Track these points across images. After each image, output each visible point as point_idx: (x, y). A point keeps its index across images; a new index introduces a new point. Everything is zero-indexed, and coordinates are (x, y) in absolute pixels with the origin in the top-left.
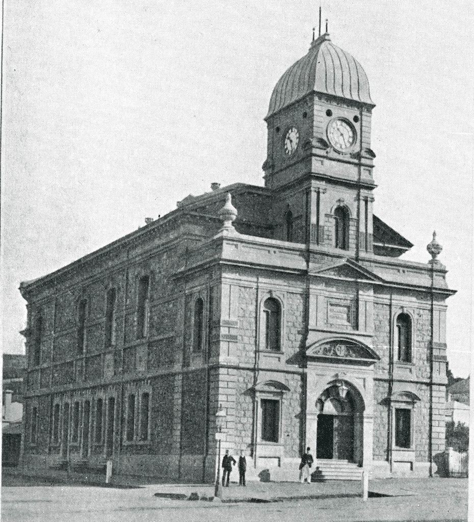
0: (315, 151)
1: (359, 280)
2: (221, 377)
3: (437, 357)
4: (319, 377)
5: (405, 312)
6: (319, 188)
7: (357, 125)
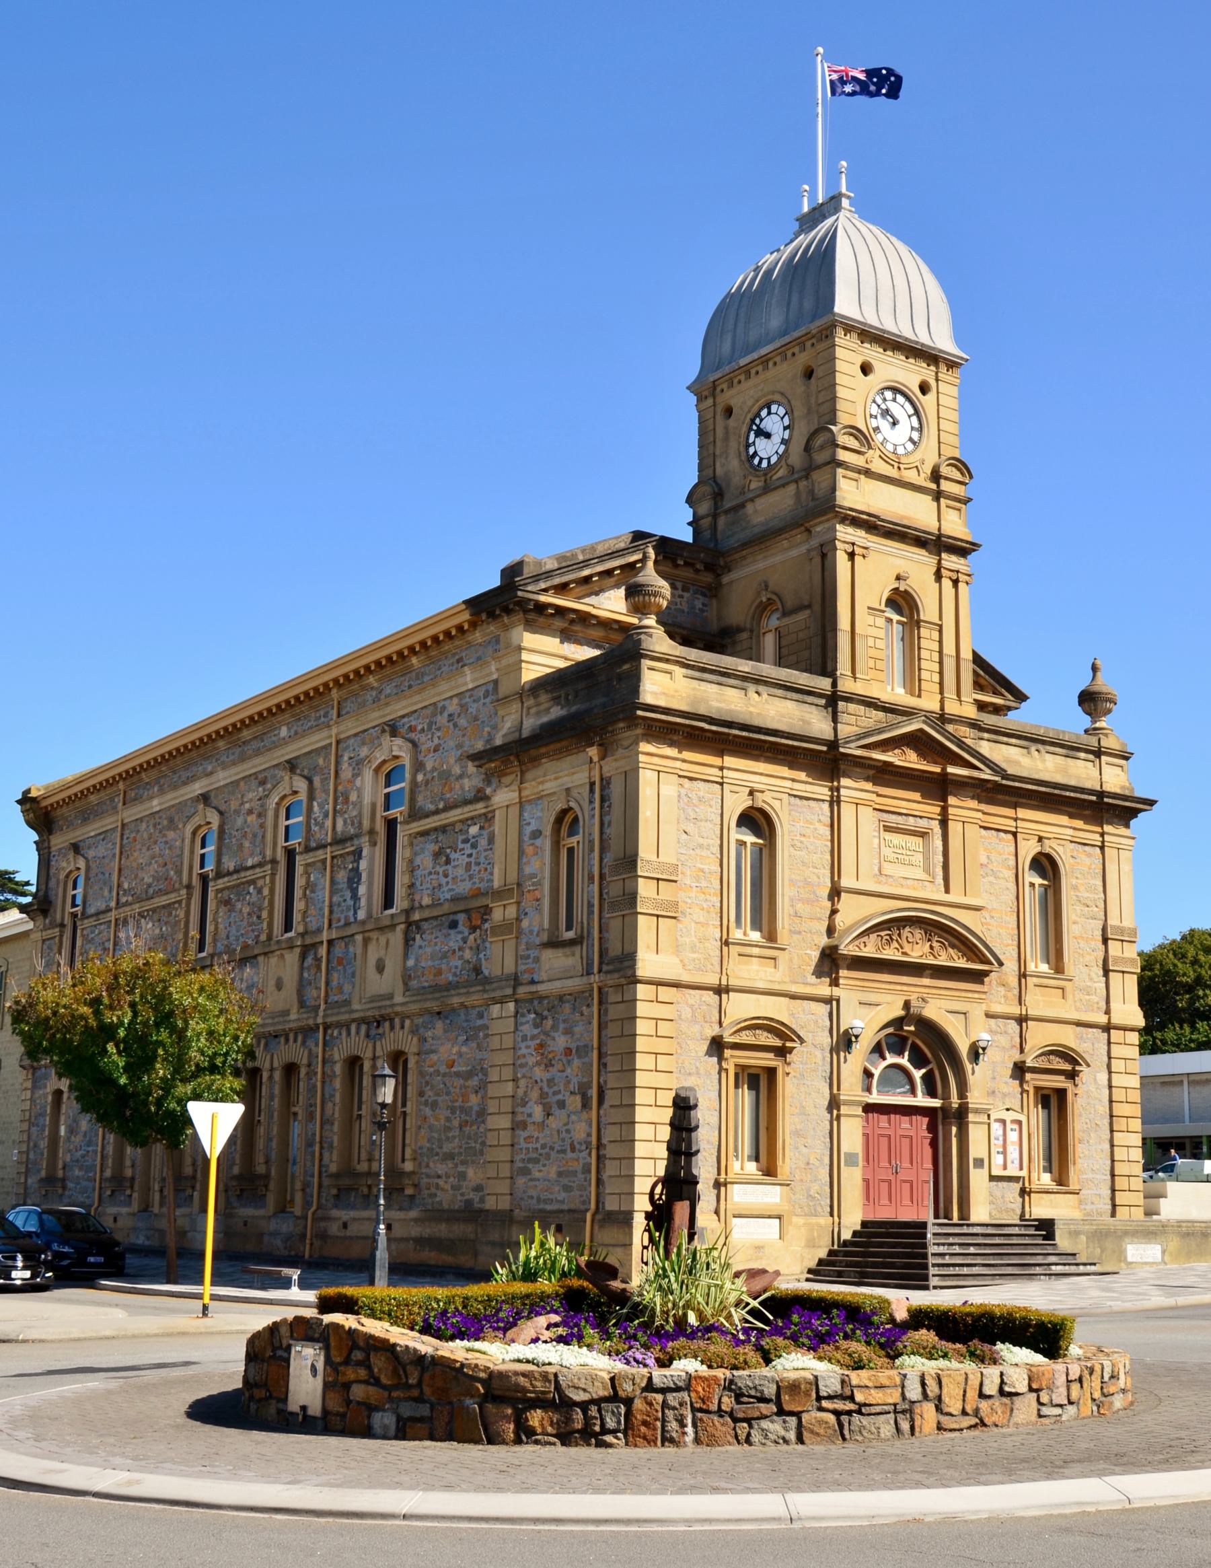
0: (842, 455)
1: (951, 770)
2: (642, 1009)
3: (1116, 959)
4: (869, 1008)
5: (1047, 850)
6: (853, 544)
7: (928, 401)
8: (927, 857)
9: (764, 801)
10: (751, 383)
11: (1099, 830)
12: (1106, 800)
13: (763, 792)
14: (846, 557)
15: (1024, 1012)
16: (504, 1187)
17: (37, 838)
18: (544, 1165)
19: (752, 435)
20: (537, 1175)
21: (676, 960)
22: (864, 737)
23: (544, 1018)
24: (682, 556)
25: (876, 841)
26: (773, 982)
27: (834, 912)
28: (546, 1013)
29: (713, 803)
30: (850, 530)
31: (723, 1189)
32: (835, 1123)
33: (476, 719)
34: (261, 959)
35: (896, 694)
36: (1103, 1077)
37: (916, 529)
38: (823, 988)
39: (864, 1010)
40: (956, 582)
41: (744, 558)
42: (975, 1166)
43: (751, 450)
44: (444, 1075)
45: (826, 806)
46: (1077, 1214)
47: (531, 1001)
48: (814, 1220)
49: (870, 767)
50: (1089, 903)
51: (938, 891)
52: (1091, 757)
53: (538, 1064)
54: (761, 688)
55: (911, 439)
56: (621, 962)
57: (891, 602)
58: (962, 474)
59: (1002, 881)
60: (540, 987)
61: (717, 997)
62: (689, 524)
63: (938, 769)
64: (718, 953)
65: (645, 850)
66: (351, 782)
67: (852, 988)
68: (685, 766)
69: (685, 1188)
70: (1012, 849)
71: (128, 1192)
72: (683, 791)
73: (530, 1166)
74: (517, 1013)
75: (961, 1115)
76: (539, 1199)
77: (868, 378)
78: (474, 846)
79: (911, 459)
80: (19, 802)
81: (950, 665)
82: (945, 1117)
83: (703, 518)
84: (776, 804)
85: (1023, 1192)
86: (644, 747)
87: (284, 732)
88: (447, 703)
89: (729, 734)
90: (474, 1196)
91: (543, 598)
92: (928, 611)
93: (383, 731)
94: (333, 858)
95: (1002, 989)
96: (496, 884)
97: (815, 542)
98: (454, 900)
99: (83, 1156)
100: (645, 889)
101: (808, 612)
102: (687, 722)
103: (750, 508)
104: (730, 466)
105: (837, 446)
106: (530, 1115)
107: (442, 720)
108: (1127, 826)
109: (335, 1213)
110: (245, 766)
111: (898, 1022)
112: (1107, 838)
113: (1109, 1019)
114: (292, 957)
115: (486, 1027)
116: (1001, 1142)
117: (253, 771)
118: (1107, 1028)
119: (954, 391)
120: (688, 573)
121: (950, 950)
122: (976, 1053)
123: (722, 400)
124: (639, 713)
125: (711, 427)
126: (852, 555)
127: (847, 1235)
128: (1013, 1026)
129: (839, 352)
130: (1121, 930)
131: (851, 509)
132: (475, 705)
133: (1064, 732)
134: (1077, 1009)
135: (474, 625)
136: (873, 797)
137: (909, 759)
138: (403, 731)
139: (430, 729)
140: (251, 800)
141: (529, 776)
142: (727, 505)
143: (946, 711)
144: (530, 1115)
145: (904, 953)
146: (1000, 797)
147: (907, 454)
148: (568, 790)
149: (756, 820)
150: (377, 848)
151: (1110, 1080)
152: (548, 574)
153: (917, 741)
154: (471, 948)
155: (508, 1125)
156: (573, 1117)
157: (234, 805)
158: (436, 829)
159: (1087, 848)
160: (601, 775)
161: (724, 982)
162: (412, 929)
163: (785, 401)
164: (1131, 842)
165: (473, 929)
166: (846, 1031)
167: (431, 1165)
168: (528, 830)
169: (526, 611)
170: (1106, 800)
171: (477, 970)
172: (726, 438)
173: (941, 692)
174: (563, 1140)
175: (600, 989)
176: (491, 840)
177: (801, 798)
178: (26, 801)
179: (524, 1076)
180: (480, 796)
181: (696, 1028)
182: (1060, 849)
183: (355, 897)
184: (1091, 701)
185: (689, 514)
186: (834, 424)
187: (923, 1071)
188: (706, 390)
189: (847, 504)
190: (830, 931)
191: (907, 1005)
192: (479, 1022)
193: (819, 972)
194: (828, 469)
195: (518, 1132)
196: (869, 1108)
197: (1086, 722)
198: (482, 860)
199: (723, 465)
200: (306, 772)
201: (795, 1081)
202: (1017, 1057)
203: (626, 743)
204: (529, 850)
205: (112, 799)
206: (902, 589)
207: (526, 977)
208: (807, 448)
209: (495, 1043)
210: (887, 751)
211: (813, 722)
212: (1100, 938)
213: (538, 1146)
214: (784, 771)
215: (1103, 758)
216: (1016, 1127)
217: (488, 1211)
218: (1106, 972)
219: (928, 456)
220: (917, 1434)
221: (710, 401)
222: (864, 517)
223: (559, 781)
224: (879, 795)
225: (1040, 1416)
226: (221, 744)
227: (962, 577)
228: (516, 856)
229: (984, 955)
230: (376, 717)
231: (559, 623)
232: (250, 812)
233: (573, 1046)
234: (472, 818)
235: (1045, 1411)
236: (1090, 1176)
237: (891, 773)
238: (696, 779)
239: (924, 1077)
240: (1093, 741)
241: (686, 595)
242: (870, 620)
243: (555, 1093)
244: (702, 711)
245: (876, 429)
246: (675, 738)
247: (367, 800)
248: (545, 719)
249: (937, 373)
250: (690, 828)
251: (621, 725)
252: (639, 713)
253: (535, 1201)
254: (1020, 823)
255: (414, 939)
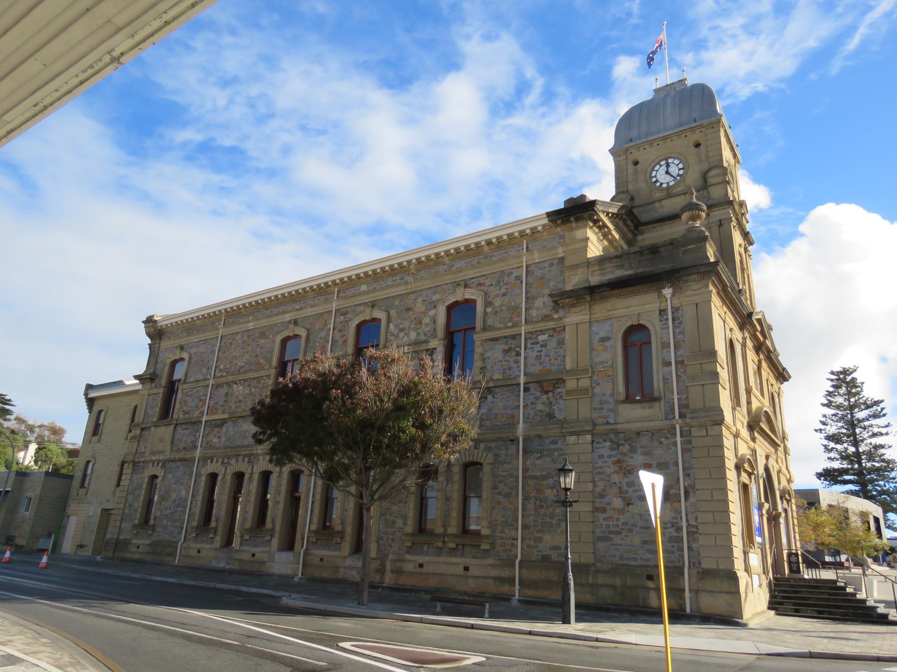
17: (150, 342)
20: (619, 542)
33: (542, 278)
53: (615, 472)
71: (211, 535)
73: (612, 536)
74: (593, 441)
76: (621, 558)
96: (568, 367)
99: (171, 513)
106: (610, 504)
109: (408, 557)
141: (594, 307)
144: (610, 504)
148: (639, 314)
155: (590, 509)
168: (596, 338)
176: (561, 343)
178: (149, 322)
179: (601, 480)
198: (552, 353)
213: (620, 523)
221: (624, 157)
234: (541, 331)
243: (634, 491)
253: (618, 558)
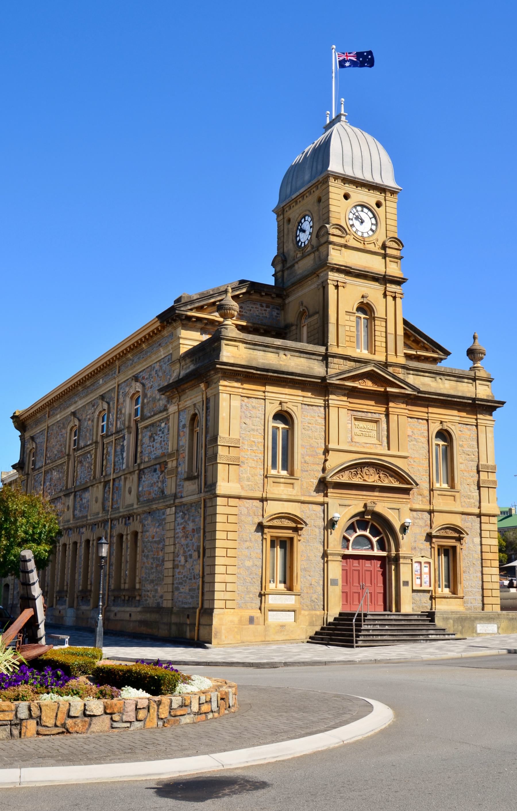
0: (332, 239)
1: (389, 389)
2: (219, 509)
3: (484, 481)
4: (344, 508)
6: (337, 281)
8: (378, 433)
9: (287, 407)
10: (297, 207)
11: (475, 417)
12: (477, 402)
13: (286, 403)
14: (334, 287)
15: (432, 508)
16: (169, 596)
17: (20, 434)
18: (184, 586)
19: (298, 232)
20: (182, 590)
21: (239, 486)
22: (340, 375)
23: (185, 514)
24: (264, 291)
25: (350, 425)
26: (294, 495)
27: (326, 460)
28: (186, 512)
29: (260, 409)
30: (336, 274)
31: (263, 597)
32: (326, 564)
34: (90, 488)
35: (363, 353)
36: (477, 540)
37: (372, 273)
38: (320, 498)
39: (343, 508)
40: (394, 298)
41: (294, 290)
42: (404, 585)
43: (298, 239)
44: (151, 542)
45: (322, 409)
46: (461, 609)
47: (181, 506)
48: (314, 612)
49: (345, 389)
50: (470, 453)
51: (384, 449)
52: (471, 381)
54: (286, 353)
55: (371, 230)
56: (211, 487)
57: (359, 309)
58: (399, 245)
59: (421, 444)
60: (183, 500)
61: (261, 503)
62: (273, 275)
63: (382, 389)
64: (262, 481)
65: (223, 432)
66: (122, 404)
67: (335, 498)
68: (244, 391)
69: (30, 602)
70: (426, 427)
72: (244, 403)
73: (179, 586)
74: (176, 512)
75: (396, 560)
77: (349, 200)
78: (163, 433)
79: (371, 239)
80: (12, 418)
81: (391, 338)
82: (389, 561)
83: (278, 272)
84: (294, 409)
85: (432, 598)
86: (222, 382)
87: (101, 382)
88: (155, 365)
89: (268, 375)
90: (159, 600)
91: (189, 313)
92: (379, 312)
93: (132, 380)
94: (116, 440)
95: (420, 497)
97: (320, 281)
98: (156, 458)
100: (222, 451)
101: (318, 315)
102: (244, 370)
103: (296, 266)
104: (290, 247)
105: (330, 234)
106: (180, 561)
107: (153, 373)
108: (491, 415)
110: (88, 398)
111: (361, 514)
112: (479, 421)
113: (480, 511)
114: (101, 486)
115: (165, 519)
116: (419, 573)
117: (90, 400)
118: (479, 515)
119: (395, 205)
120: (268, 299)
121: (390, 478)
122: (404, 528)
123: (287, 215)
124: (218, 366)
125: (282, 229)
126: (337, 287)
127: (331, 620)
128: (426, 515)
129: (331, 189)
130: (488, 467)
131: (335, 264)
132: (165, 366)
133: (455, 369)
134: (462, 506)
135: (163, 327)
136: (348, 404)
137: (368, 385)
138: (140, 379)
139: (149, 378)
140: (90, 414)
141: (182, 398)
142: (288, 265)
143: (388, 361)
145: (364, 480)
146: (419, 402)
147: (369, 236)
149: (284, 416)
150: (132, 435)
151: (481, 541)
152: (192, 302)
153: (371, 376)
154: (161, 481)
155: (171, 566)
156: (195, 563)
157: (84, 416)
158: (150, 425)
159: (468, 426)
160: (206, 397)
161: (264, 496)
162: (141, 472)
163: (310, 214)
164: (493, 423)
165: (162, 472)
166: (331, 519)
167: (146, 586)
168: (182, 424)
169: (182, 320)
170: (477, 402)
171: (163, 492)
172: (288, 234)
173: (386, 352)
174: (191, 574)
175: (204, 500)
177: (308, 405)
178: (14, 418)
180: (165, 409)
181: (250, 518)
182: (453, 427)
183: (123, 459)
184: (473, 354)
185: (272, 271)
186: (328, 224)
187: (378, 538)
188: (280, 211)
189: (334, 262)
190: (324, 470)
191: (365, 506)
192: (163, 517)
193: (318, 490)
194: (325, 245)
195: (176, 570)
196: (345, 557)
197: (470, 364)
198: (165, 439)
199: (287, 247)
200: (108, 400)
201: (304, 544)
202: (428, 530)
203: (215, 381)
204: (181, 434)
205: (45, 415)
206: (365, 302)
207: (179, 495)
208: (317, 236)
209: (168, 527)
210: (356, 381)
211: (317, 368)
212: (476, 471)
213: (182, 576)
214: (299, 392)
215: (477, 382)
216: (427, 565)
217: (164, 608)
218: (479, 488)
219: (381, 237)
220: (22, 737)
221: (282, 217)
222: (343, 268)
223: (192, 400)
224: (350, 403)
225: (113, 728)
226: (80, 388)
227: (397, 295)
228: (177, 437)
229: (408, 480)
230: (131, 373)
231: (199, 325)
232: (89, 419)
233: (195, 528)
235: (115, 725)
236: (470, 589)
237: (357, 392)
238: (251, 397)
239: (378, 541)
240: (472, 374)
241: (268, 309)
242: (347, 317)
244: (254, 364)
245: (352, 225)
246: (239, 378)
247: (127, 413)
248: (188, 371)
249: (385, 197)
250: (247, 421)
251: (212, 372)
252: (218, 366)
253: (181, 603)
254: (430, 415)
255: (142, 478)
